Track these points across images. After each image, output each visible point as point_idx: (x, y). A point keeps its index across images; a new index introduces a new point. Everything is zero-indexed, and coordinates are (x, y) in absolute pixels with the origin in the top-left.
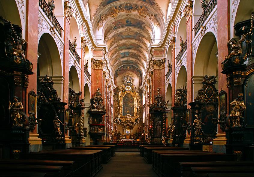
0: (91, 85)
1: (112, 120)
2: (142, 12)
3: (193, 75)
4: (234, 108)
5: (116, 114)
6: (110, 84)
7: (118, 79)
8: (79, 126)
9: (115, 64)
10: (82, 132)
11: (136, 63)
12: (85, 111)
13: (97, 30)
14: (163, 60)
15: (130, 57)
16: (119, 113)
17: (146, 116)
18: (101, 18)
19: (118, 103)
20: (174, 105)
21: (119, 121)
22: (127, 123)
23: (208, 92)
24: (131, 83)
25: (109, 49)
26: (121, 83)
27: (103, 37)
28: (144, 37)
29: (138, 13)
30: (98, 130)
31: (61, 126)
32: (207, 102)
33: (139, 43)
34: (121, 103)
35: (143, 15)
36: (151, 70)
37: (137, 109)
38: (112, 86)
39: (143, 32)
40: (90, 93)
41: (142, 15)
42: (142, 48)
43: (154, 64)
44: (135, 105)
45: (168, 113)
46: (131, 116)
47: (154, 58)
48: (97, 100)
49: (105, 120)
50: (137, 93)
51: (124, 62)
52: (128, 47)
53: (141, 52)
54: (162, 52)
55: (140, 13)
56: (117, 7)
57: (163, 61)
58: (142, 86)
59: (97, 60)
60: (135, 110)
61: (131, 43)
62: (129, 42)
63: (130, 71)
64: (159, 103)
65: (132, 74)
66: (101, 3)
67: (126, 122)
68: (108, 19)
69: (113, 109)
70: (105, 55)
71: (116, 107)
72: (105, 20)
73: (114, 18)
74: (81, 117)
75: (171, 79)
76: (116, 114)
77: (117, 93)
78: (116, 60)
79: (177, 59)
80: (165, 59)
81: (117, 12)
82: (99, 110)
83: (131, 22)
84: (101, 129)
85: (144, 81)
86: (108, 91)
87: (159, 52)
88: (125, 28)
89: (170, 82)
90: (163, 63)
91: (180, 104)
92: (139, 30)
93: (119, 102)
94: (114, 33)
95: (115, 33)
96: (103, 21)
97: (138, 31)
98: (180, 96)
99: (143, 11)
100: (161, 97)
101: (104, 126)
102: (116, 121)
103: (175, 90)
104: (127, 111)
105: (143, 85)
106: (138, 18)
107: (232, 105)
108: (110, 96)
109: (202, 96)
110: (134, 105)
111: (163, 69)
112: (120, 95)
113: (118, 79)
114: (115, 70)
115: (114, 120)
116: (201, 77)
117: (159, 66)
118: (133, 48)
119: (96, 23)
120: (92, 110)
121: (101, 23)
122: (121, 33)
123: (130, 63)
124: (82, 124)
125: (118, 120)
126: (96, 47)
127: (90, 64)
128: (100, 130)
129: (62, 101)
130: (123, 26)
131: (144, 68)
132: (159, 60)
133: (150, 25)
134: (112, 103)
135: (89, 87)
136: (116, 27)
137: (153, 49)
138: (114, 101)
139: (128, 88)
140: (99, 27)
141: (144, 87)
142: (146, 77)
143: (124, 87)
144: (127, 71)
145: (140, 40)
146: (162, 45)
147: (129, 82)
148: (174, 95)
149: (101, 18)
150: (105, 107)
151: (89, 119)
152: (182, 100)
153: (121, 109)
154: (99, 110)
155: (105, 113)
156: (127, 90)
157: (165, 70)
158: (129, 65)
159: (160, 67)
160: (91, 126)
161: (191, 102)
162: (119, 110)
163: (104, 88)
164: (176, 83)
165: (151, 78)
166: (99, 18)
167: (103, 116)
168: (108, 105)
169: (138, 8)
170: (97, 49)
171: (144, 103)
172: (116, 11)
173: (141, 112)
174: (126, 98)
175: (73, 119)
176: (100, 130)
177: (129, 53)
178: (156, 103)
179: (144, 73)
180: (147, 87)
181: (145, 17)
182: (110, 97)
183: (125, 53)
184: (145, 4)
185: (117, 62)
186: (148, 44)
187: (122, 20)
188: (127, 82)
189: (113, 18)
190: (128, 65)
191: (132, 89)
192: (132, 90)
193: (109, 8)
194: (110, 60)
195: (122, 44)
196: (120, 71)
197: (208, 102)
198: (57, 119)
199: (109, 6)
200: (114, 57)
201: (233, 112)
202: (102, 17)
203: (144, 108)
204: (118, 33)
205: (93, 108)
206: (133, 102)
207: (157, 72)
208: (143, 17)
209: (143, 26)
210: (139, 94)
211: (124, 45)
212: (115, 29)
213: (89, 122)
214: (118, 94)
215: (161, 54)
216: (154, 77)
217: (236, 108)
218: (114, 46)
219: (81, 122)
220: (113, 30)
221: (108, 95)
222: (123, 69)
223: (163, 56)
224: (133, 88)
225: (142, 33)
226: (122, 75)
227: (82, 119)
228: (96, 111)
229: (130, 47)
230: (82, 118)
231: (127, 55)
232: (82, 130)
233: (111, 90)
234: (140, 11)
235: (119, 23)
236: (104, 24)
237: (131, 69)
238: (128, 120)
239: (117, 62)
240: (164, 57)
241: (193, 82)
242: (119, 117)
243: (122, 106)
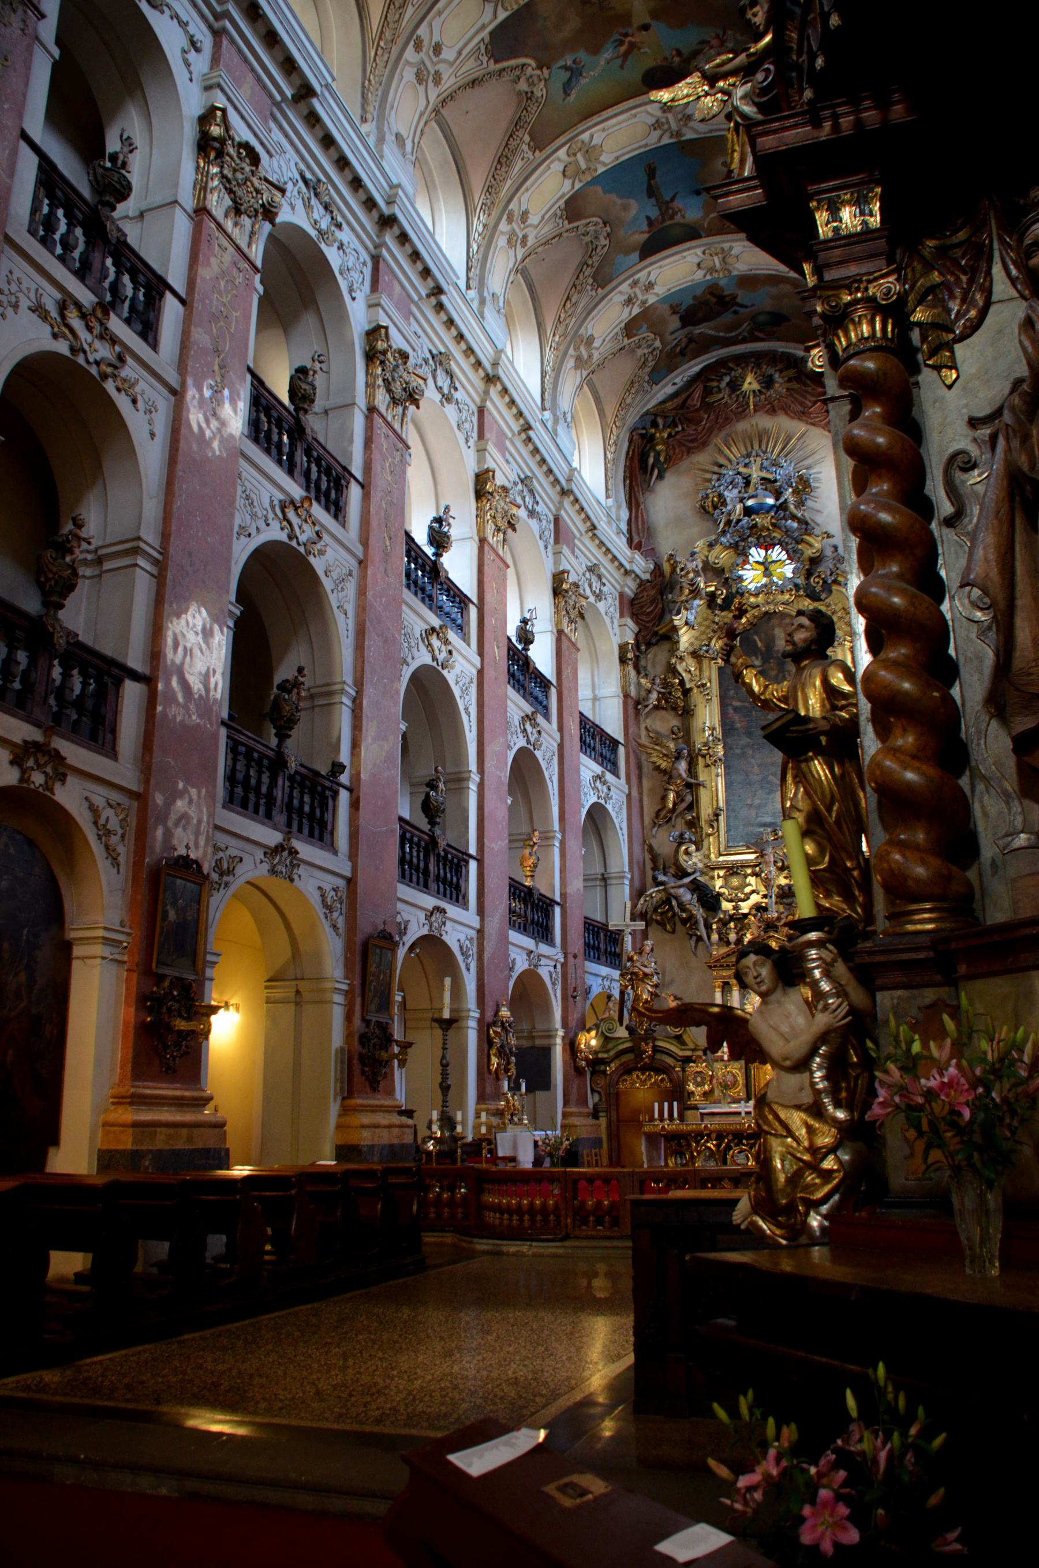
5: (663, 840)
19: (675, 722)
71: (664, 765)
93: (687, 713)
125: (687, 896)
139: (766, 566)
147: (770, 501)
153: (703, 776)
162: (693, 787)
191: (809, 574)
222: (706, 406)
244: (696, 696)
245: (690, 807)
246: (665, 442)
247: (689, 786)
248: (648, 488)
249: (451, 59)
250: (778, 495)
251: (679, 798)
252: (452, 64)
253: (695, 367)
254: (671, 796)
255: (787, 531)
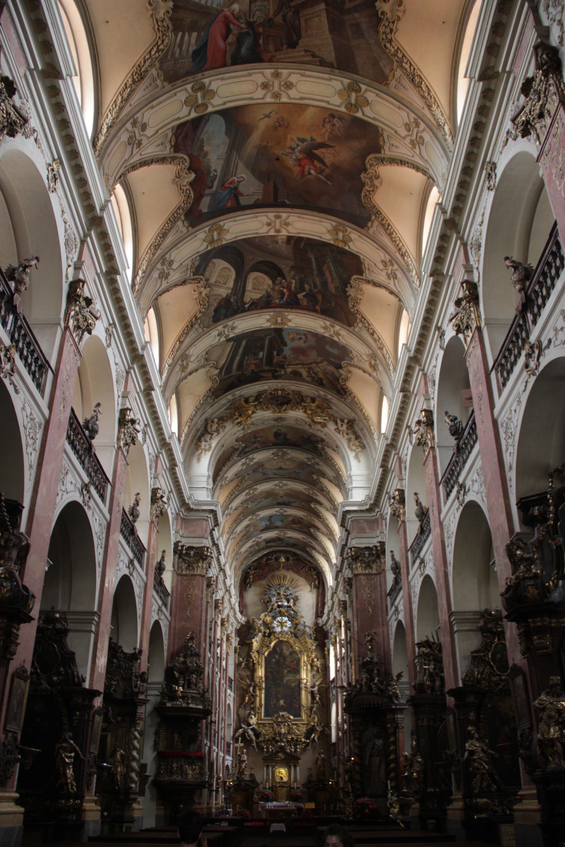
0: (170, 623)
1: (229, 733)
2: (316, 412)
3: (453, 609)
4: (544, 715)
6: (226, 612)
7: (252, 595)
8: (127, 759)
9: (243, 549)
10: (133, 781)
11: (304, 547)
12: (144, 711)
13: (195, 461)
14: (379, 548)
15: (287, 527)
16: (253, 709)
17: (340, 721)
18: (206, 427)
19: (249, 673)
20: (415, 689)
21: (254, 738)
22: (277, 742)
23: (498, 656)
24: (290, 607)
25: (226, 507)
26: (260, 608)
27: (211, 481)
28: (324, 475)
29: (305, 415)
30: (183, 773)
31: (78, 764)
32: (499, 684)
33: (311, 492)
34: (261, 672)
35: (318, 419)
36: (347, 573)
37: (312, 693)
38: (232, 619)
39: (321, 463)
40: (165, 647)
41: (316, 420)
42: (321, 504)
43: (355, 558)
44: (305, 681)
45: (401, 713)
46: (292, 717)
47: (354, 543)
48: (186, 671)
49: (207, 734)
50: (309, 641)
51: (268, 541)
52: (280, 500)
53: (318, 515)
54: (374, 523)
55: (312, 414)
56: (251, 399)
57: (377, 550)
58: (325, 618)
59: (191, 548)
60: (305, 698)
61: (289, 489)
62: (281, 487)
63: (288, 570)
64: (372, 679)
65: (293, 580)
66: (210, 390)
67: (274, 739)
68: (227, 430)
69: (232, 694)
70: (213, 530)
71: (245, 687)
72: (216, 434)
73: (242, 427)
74: (136, 730)
75: (401, 607)
76: (241, 712)
77: (248, 642)
78: (247, 536)
79: (413, 552)
80: (382, 544)
81: (250, 412)
82: (188, 704)
83: (289, 437)
84: (193, 770)
85: (329, 603)
86: (218, 636)
87: (365, 525)
88: (272, 452)
89: (401, 617)
90: (378, 557)
91: (433, 689)
92: (310, 456)
93: (253, 671)
94: (240, 463)
95: (243, 464)
96: (212, 434)
97: (306, 460)
98: (430, 661)
99: (318, 410)
100: (377, 663)
101: (201, 758)
102: (243, 735)
103: (413, 642)
104: (278, 700)
105: (328, 615)
106: (307, 428)
107: (538, 706)
108: (224, 652)
109: (483, 670)
110: (299, 681)
111: (380, 574)
112: (255, 644)
113: (252, 595)
114: (243, 567)
115: (236, 731)
116: (475, 613)
117: (368, 566)
118: (294, 504)
119: (192, 440)
120: (169, 705)
121: (206, 441)
122: (260, 465)
123: (288, 545)
124: (135, 753)
125: (251, 733)
126: (189, 509)
127: (169, 564)
128: (190, 772)
129: (87, 685)
130: (265, 446)
131: (328, 560)
132: (367, 548)
133: (337, 447)
134: (231, 673)
135: (164, 629)
136: (247, 450)
137: (349, 516)
138: (238, 666)
139: (282, 624)
140: (200, 451)
141: (331, 622)
142: (334, 593)
143: (268, 619)
144: (278, 569)
145: (314, 484)
146: (371, 505)
147: (286, 604)
148: (414, 659)
149: (206, 427)
150: (207, 695)
151: (157, 733)
152: (437, 674)
153: (258, 693)
154: (188, 704)
155: (207, 712)
156: (278, 629)
157: (385, 576)
158: (285, 552)
159: (371, 568)
160: (161, 757)
161: (454, 687)
162: (254, 696)
163: (208, 629)
164: (415, 621)
165: (349, 597)
166: (203, 428)
167: (199, 725)
168: (217, 683)
169: (305, 402)
170: (192, 513)
171: (332, 675)
172: (247, 410)
173: (323, 704)
174: (275, 658)
175: (109, 738)
176: (191, 773)
177: (283, 517)
178: (365, 680)
179: (330, 581)
180: (340, 622)
181: (324, 425)
182: (224, 656)
183: (271, 517)
184: (322, 393)
185: (250, 544)
186: (339, 498)
187: (263, 430)
188: (279, 606)
189: (237, 428)
190: (280, 551)
191: (295, 628)
192: (292, 631)
193: (229, 402)
194: (228, 539)
195: (262, 493)
196: (255, 569)
197: (500, 687)
198: (67, 742)
199: (230, 397)
200: (239, 529)
201: (542, 726)
202: (209, 426)
203: (334, 692)
204: (252, 463)
205: (173, 696)
206: (297, 670)
207: (364, 582)
208: (319, 427)
209: (320, 446)
210: (317, 642)
211: (269, 494)
212: (244, 453)
213: (156, 744)
214: (250, 645)
215: (372, 529)
216: (357, 599)
217: (550, 717)
218: (242, 497)
219: (135, 748)
220: (238, 456)
221: (218, 650)
223: (378, 537)
224: (297, 624)
225: (318, 464)
226: (264, 582)
227: (136, 738)
228: (181, 709)
229: (286, 499)
230: (136, 734)
231: (279, 524)
232: (134, 775)
233: (229, 632)
234: (311, 410)
235: (255, 438)
236: (213, 445)
237: (291, 561)
238: (283, 731)
239: (250, 544)
240: (379, 539)
241: (455, 629)
242: (253, 720)
243: (264, 686)
244: (256, 666)
245: (253, 703)
246: (253, 575)
247: (253, 695)
248: (246, 590)
249: (149, 136)
250: (288, 601)
251: (250, 699)
252: (148, 138)
253: (265, 552)
254: (247, 698)
255: (290, 614)
